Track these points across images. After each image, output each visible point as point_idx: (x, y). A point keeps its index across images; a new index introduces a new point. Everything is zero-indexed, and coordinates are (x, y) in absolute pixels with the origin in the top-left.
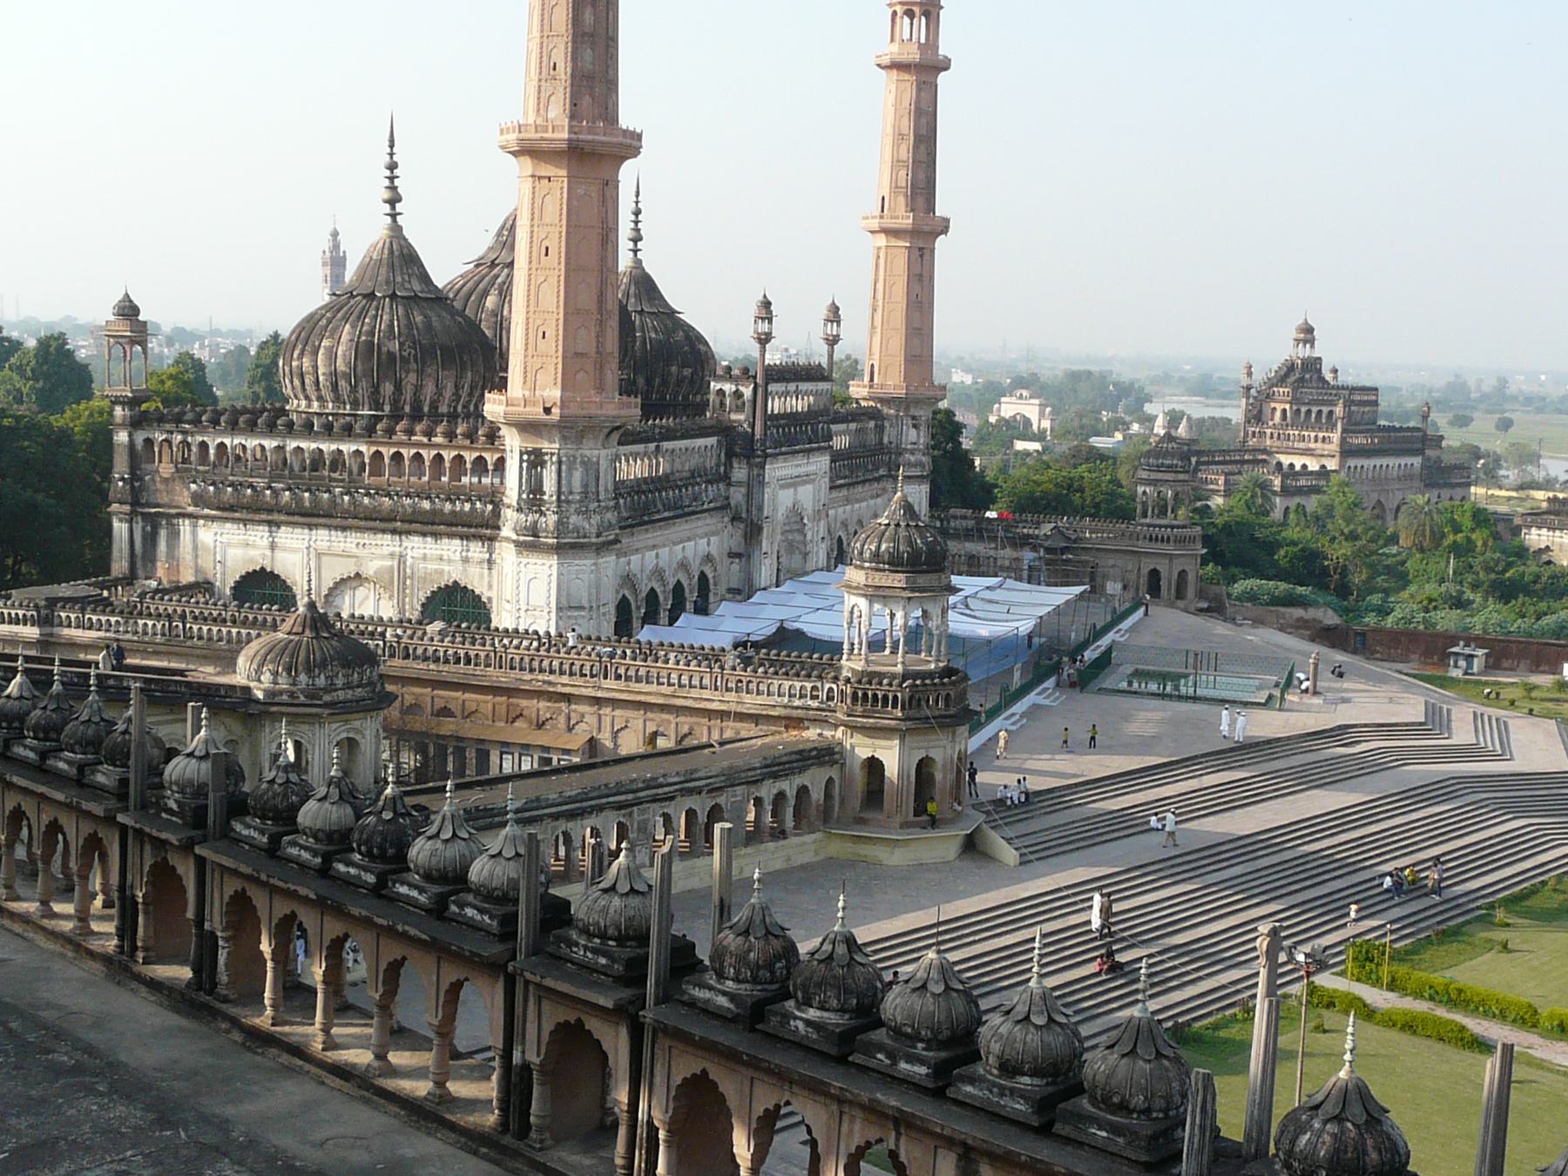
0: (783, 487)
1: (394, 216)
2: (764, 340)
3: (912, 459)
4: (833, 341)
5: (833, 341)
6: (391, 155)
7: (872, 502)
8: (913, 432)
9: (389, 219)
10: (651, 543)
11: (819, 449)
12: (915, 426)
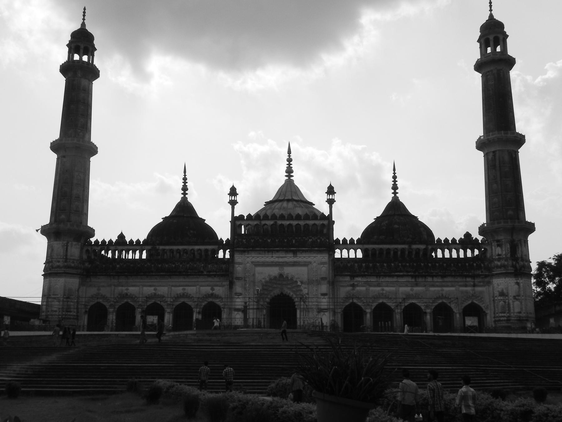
0: (257, 264)
1: (185, 194)
2: (233, 203)
3: (499, 264)
4: (331, 202)
5: (331, 202)
6: (185, 175)
7: (469, 289)
8: (498, 250)
9: (183, 196)
10: (149, 284)
11: (305, 251)
12: (498, 245)
